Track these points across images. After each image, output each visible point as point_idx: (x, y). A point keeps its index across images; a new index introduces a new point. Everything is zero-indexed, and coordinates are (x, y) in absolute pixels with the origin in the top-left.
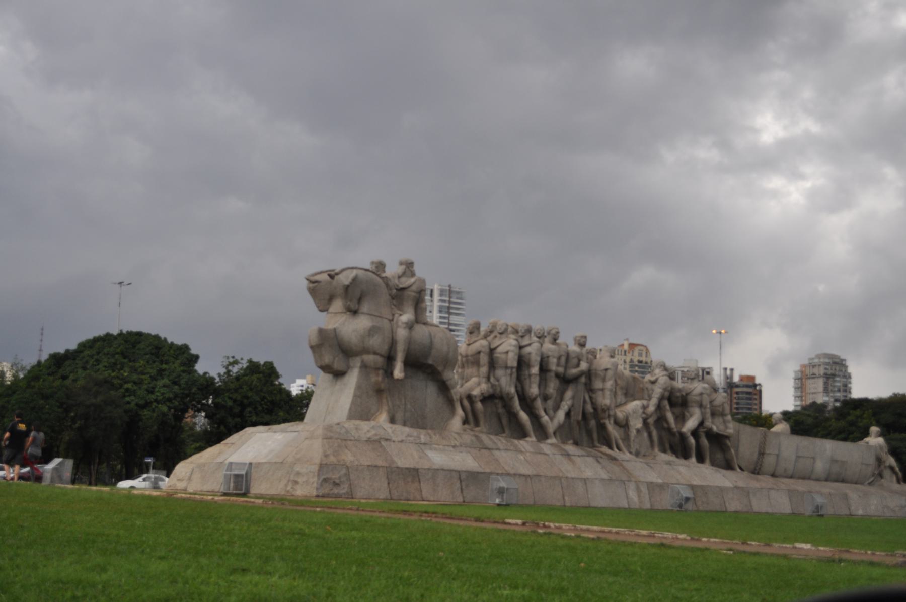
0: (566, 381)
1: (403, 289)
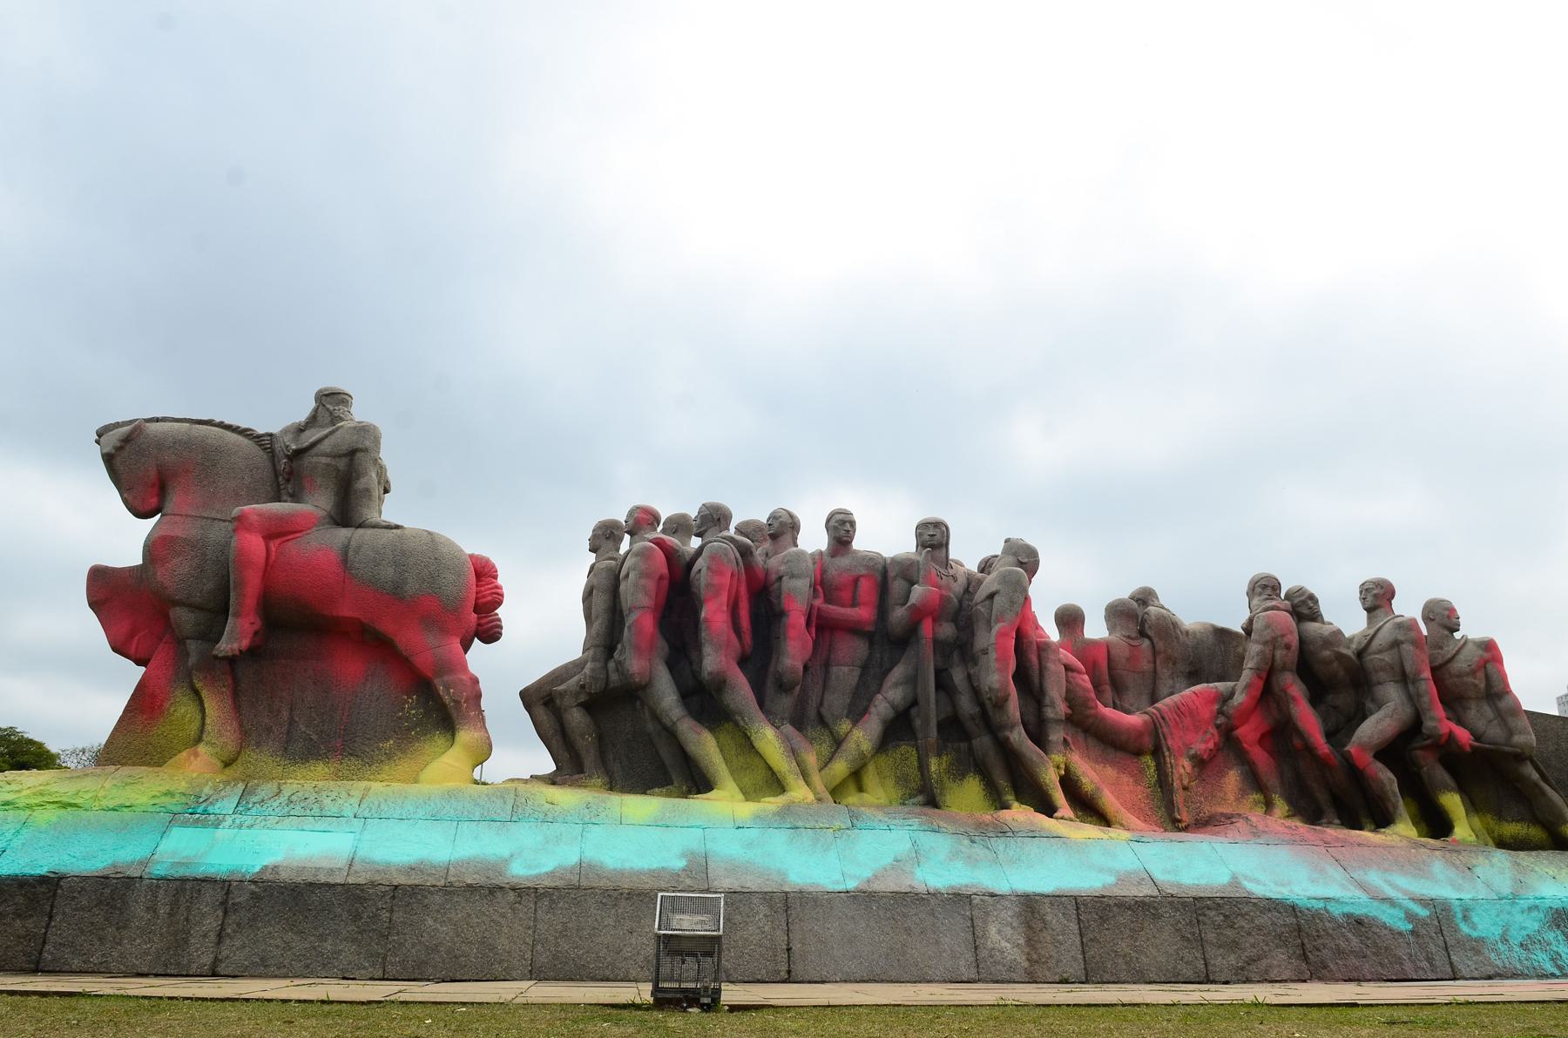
0: (889, 641)
1: (299, 453)
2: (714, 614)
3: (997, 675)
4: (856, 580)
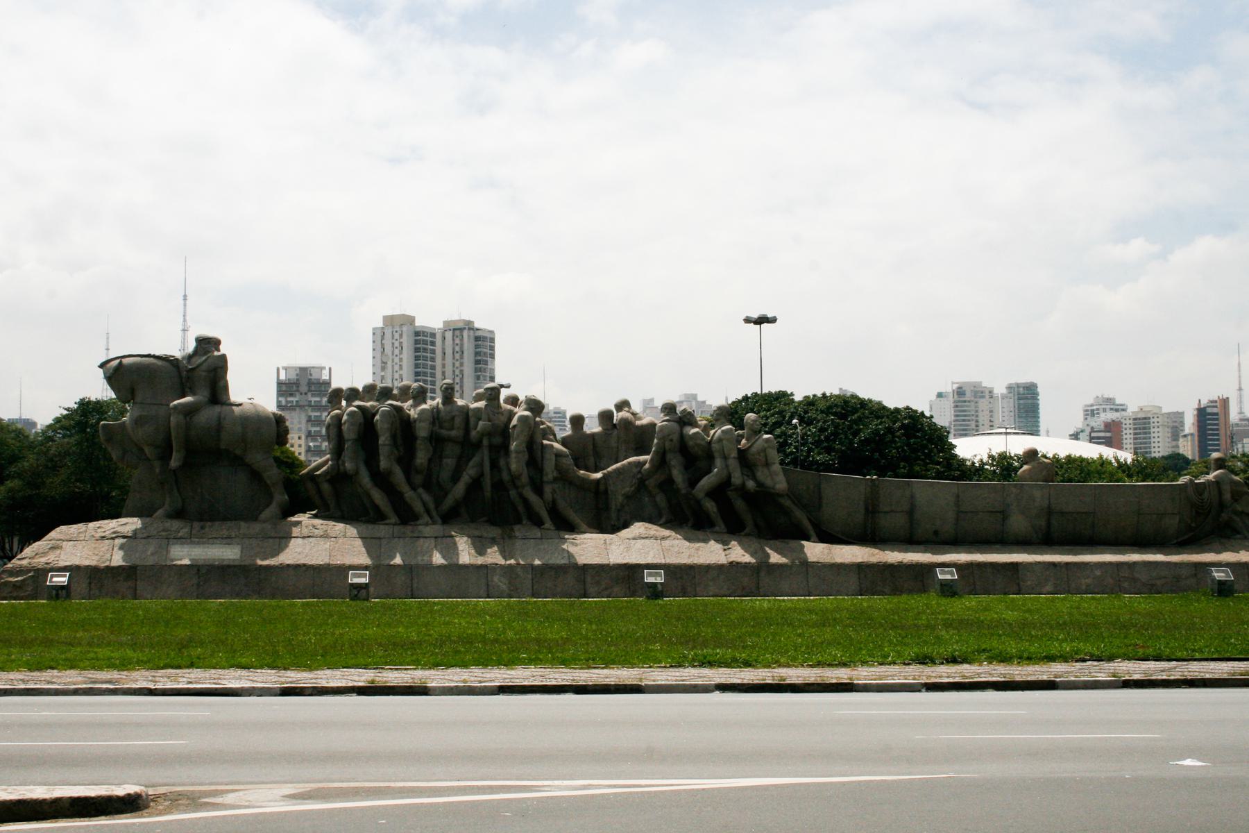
0: (468, 446)
2: (383, 439)
3: (516, 463)
4: (453, 418)
